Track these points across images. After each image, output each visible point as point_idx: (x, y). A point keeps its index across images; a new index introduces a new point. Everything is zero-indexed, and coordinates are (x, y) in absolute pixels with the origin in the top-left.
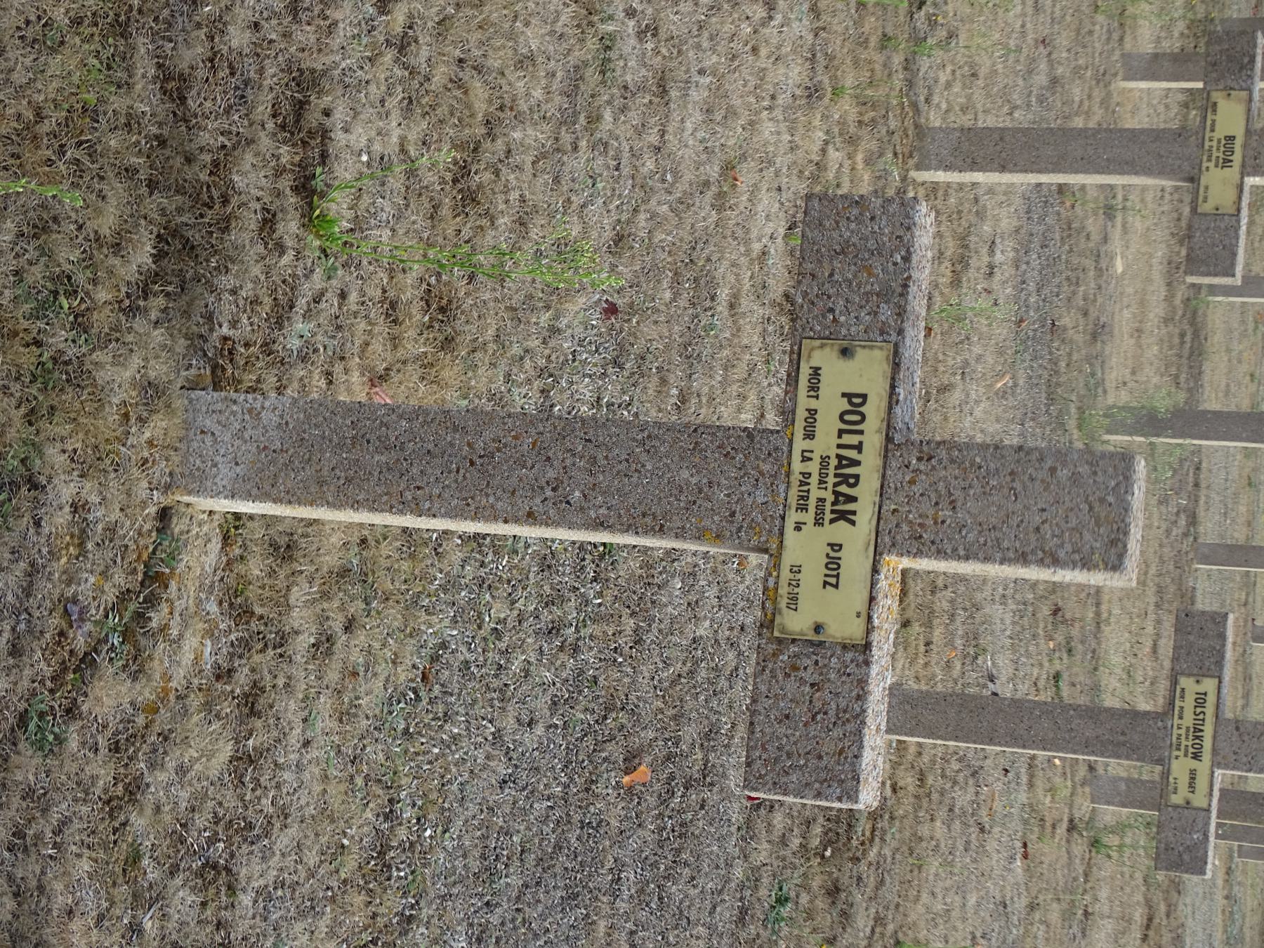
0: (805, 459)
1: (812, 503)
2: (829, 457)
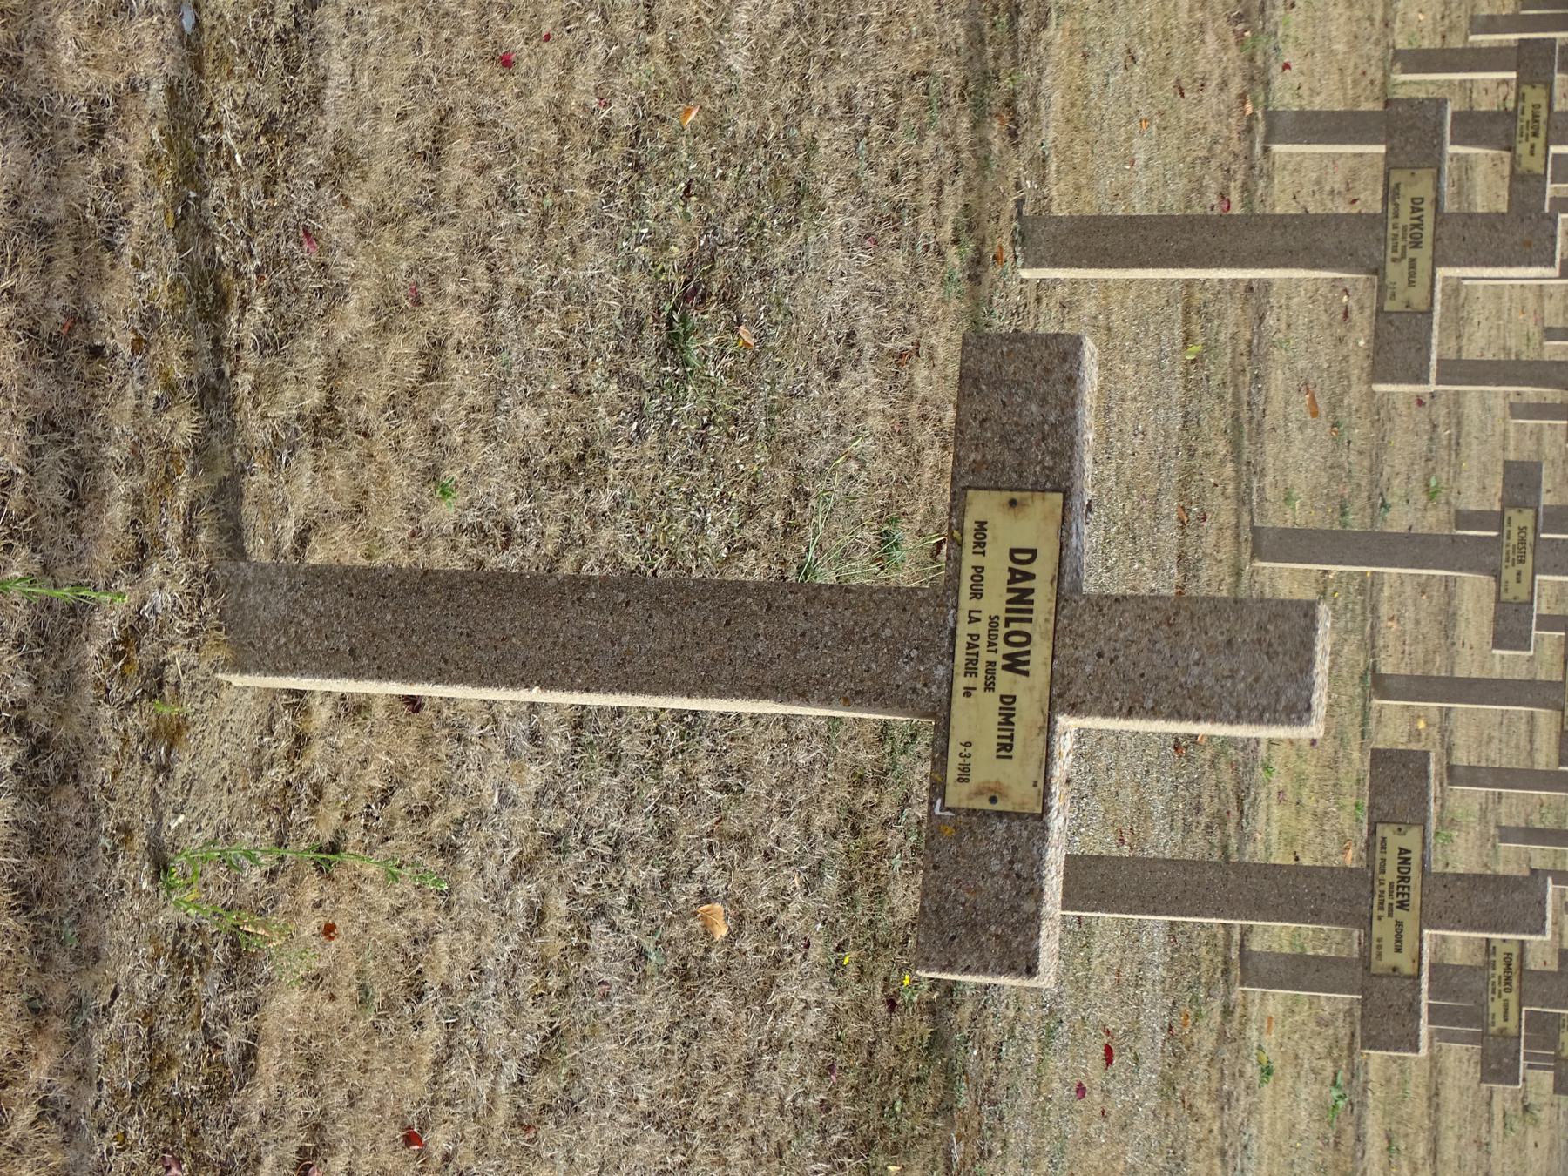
0: (973, 620)
1: (982, 667)
2: (997, 617)
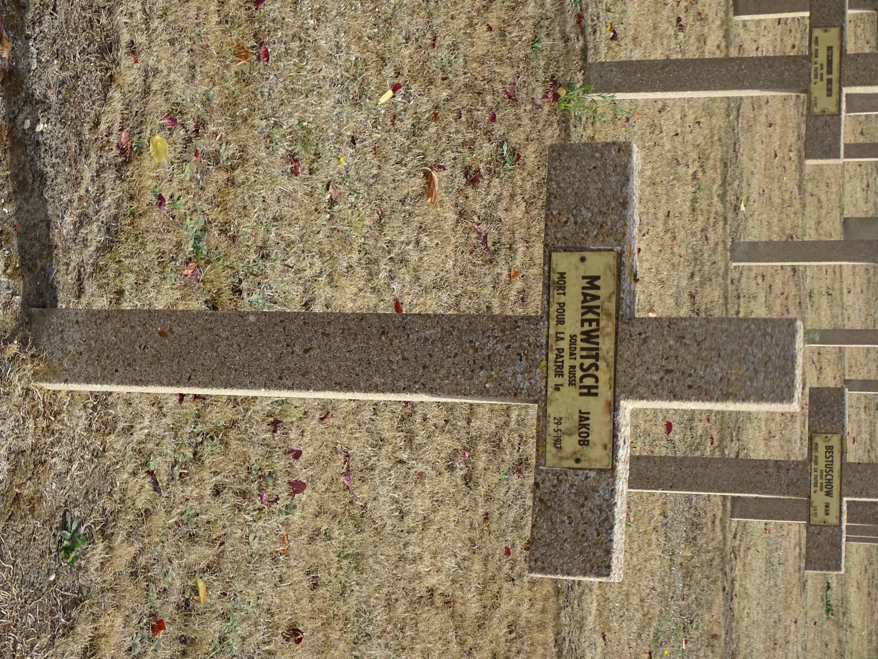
0: (559, 339)
1: (566, 370)
